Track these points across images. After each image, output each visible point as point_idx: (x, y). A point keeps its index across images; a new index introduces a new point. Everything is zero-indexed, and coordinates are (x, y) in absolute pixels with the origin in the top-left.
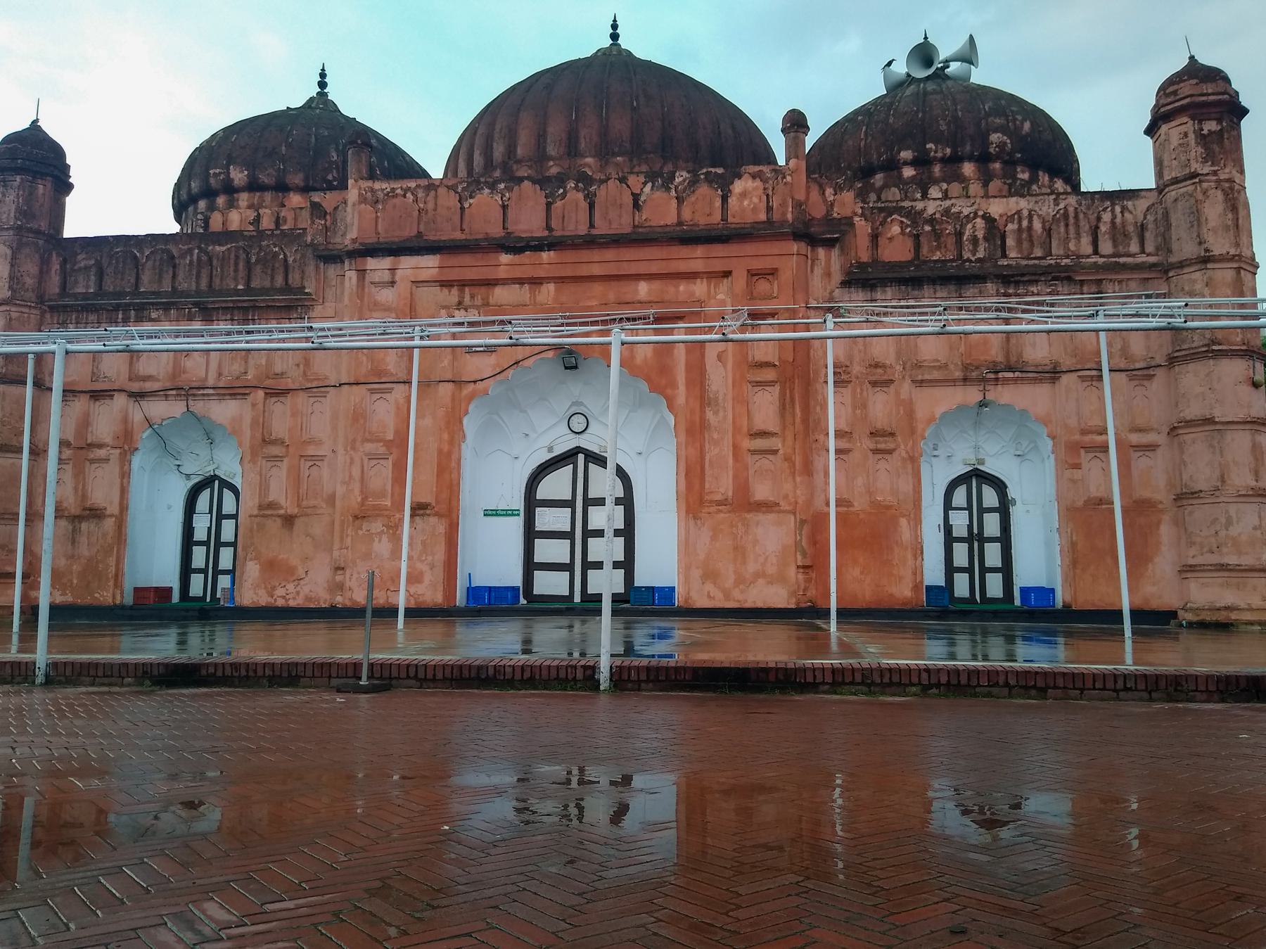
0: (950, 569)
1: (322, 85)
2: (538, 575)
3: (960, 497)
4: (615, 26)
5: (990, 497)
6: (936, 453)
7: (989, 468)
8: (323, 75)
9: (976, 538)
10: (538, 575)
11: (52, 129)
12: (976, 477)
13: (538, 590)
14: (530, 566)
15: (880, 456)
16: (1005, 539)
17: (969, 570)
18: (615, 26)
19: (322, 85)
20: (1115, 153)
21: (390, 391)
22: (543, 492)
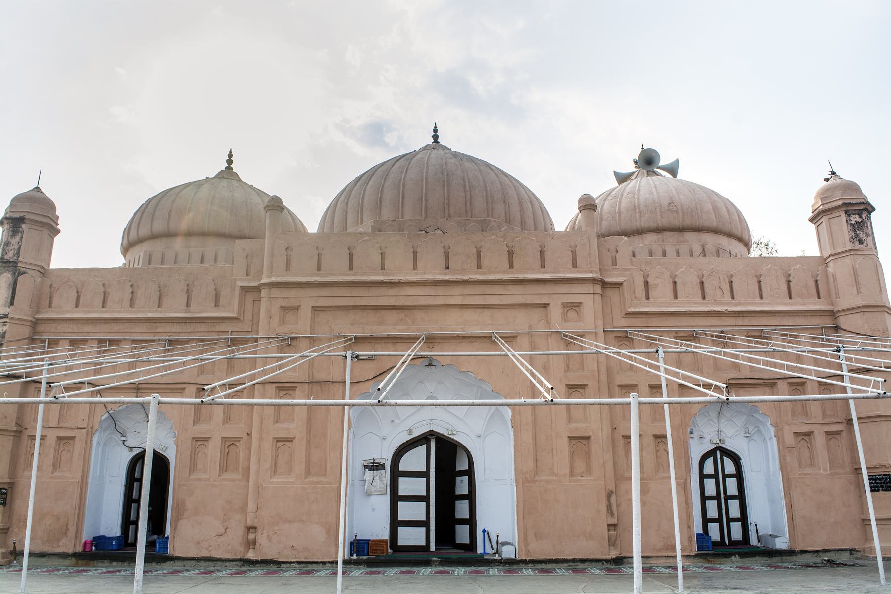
0: (706, 521)
1: (230, 162)
2: (401, 530)
3: (709, 468)
4: (435, 130)
5: (730, 468)
6: (692, 435)
7: (728, 445)
8: (230, 155)
9: (721, 498)
10: (401, 530)
11: (49, 192)
12: (720, 452)
13: (401, 542)
14: (395, 523)
15: (659, 440)
16: (741, 497)
17: (719, 520)
18: (435, 130)
19: (230, 162)
20: (785, 230)
21: (294, 388)
22: (402, 467)
